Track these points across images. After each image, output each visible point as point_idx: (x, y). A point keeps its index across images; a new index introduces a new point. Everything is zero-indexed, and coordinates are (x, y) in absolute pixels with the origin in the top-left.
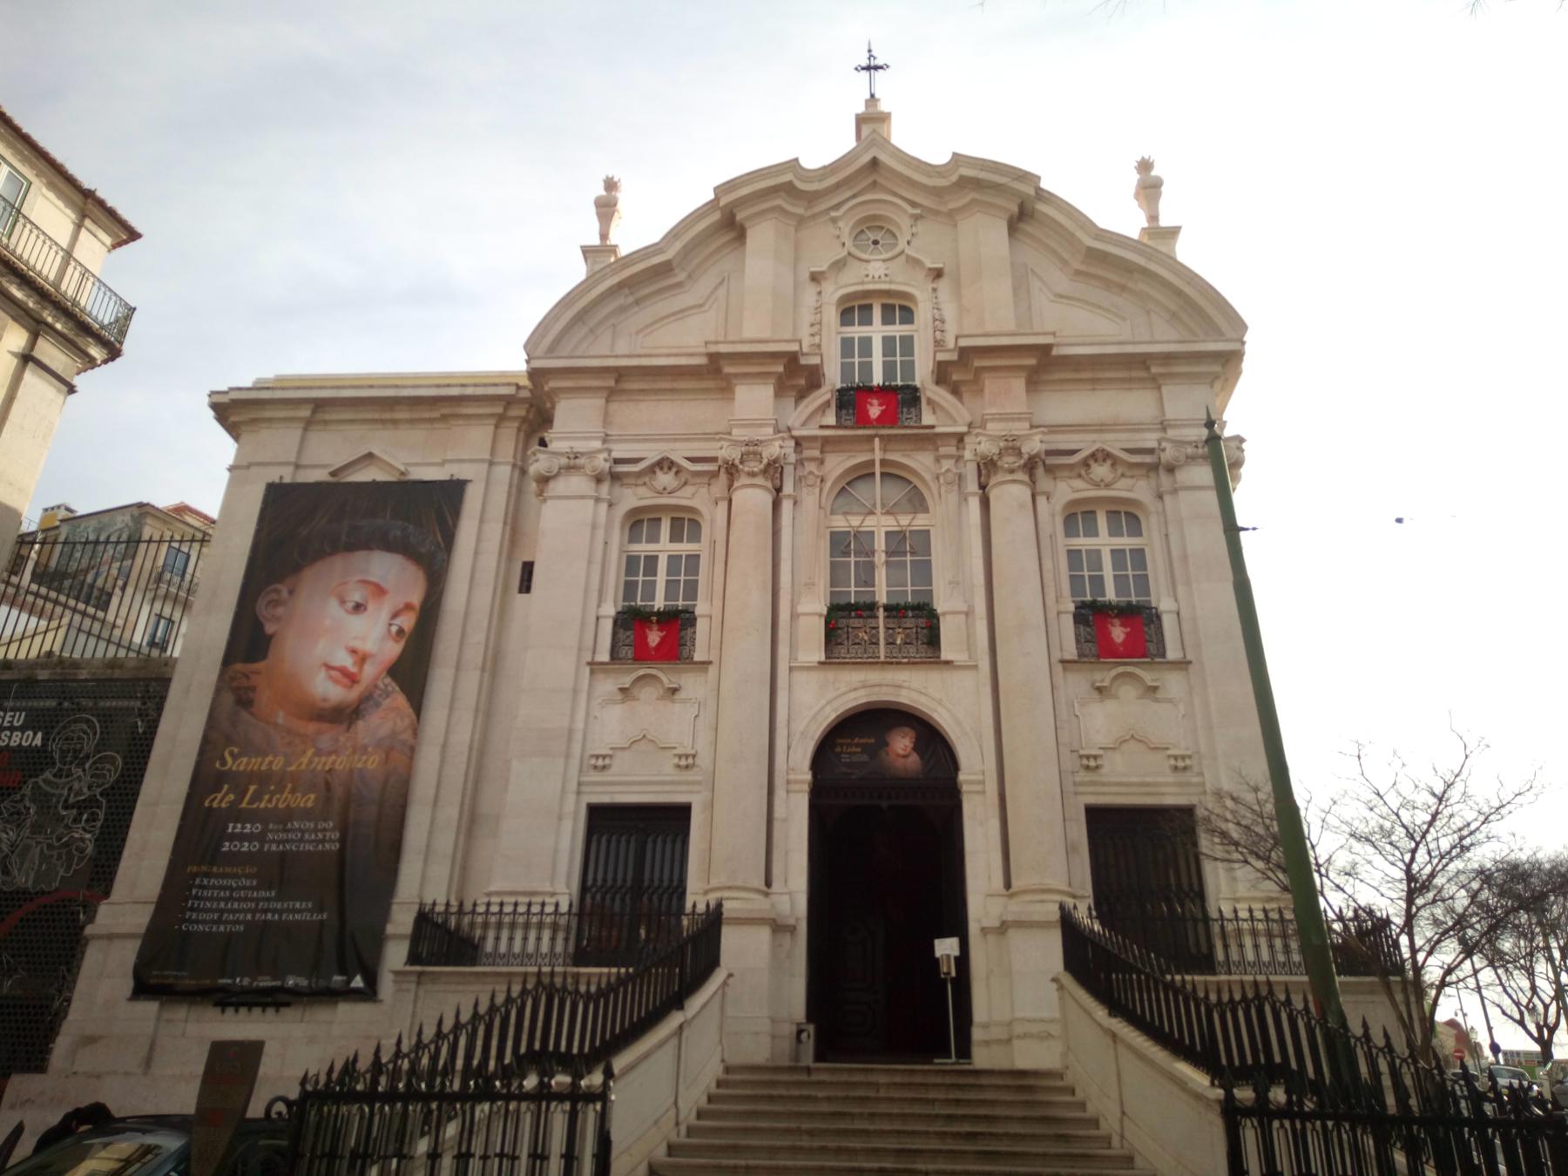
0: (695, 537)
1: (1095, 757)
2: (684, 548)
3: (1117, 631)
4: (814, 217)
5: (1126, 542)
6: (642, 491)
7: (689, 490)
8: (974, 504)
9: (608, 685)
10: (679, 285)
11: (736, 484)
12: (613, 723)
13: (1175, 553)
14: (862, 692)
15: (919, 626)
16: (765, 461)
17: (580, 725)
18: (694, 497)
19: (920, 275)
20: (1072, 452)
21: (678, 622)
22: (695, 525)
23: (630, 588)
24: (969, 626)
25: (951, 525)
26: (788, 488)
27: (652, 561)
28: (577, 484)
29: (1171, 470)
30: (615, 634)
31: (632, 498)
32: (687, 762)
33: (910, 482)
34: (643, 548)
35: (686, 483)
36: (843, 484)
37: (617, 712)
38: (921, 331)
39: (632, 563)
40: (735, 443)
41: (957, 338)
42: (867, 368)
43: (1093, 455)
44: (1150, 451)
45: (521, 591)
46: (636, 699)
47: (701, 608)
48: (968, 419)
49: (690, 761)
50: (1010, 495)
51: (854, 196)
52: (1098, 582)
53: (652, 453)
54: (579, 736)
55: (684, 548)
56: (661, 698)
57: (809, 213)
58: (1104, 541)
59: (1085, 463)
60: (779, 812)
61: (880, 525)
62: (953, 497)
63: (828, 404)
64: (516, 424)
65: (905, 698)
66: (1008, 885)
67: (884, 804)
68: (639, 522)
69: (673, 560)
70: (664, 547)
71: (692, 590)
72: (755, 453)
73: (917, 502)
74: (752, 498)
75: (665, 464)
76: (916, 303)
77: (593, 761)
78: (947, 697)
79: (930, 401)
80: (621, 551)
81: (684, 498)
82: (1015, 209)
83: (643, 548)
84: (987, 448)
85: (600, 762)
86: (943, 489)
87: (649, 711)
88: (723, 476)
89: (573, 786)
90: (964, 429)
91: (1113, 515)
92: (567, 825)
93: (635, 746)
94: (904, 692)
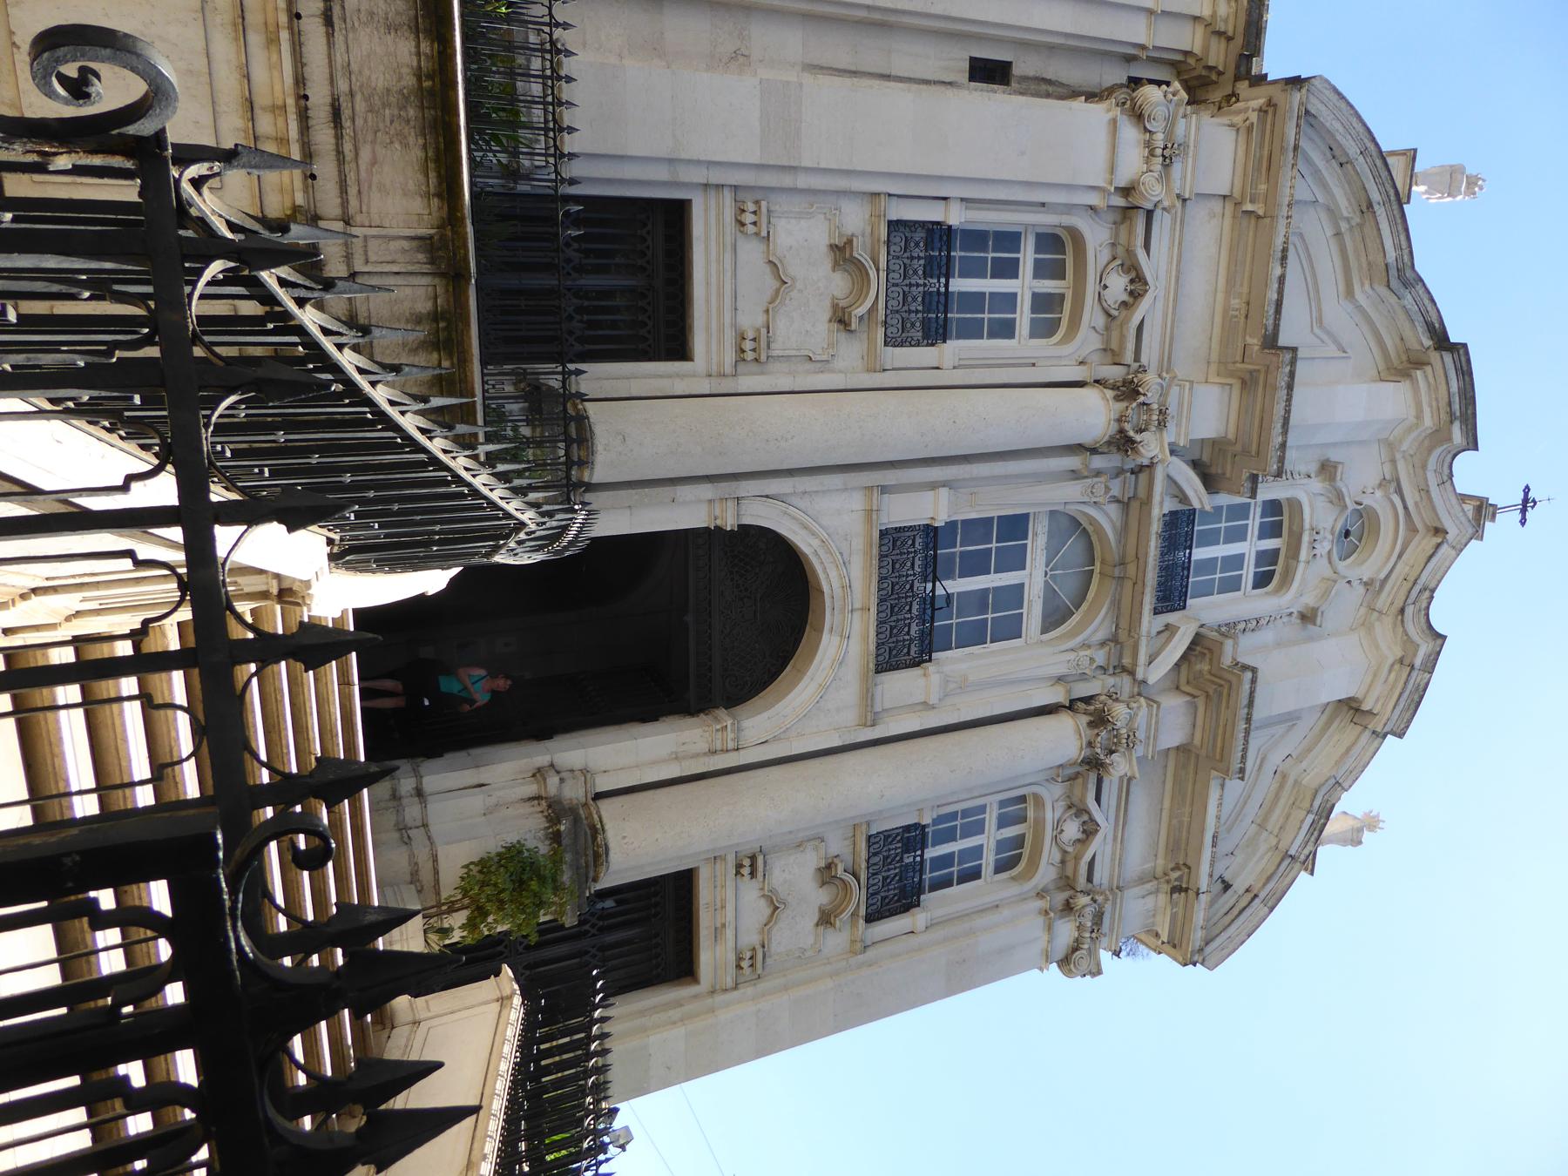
1: (753, 874)
2: (1023, 316)
3: (897, 873)
4: (1393, 461)
5: (988, 861)
6: (1105, 256)
7: (1100, 321)
8: (1056, 695)
9: (855, 219)
10: (1350, 293)
11: (1110, 394)
13: (979, 922)
14: (836, 584)
15: (909, 636)
16: (1138, 438)
17: (802, 181)
19: (1309, 600)
20: (1098, 799)
21: (930, 319)
23: (976, 238)
24: (912, 708)
25: (1030, 664)
29: (1068, 908)
30: (923, 224)
31: (1097, 237)
32: (752, 350)
33: (1078, 607)
34: (1028, 256)
35: (1109, 315)
36: (1085, 524)
38: (1246, 603)
39: (1010, 240)
40: (1164, 394)
41: (1254, 670)
42: (1211, 539)
43: (1092, 820)
44: (1090, 879)
45: (973, 60)
46: (836, 266)
47: (953, 349)
48: (1152, 680)
49: (750, 356)
50: (1062, 739)
51: (1406, 508)
52: (949, 836)
53: (1155, 266)
54: (787, 180)
55: (1023, 316)
56: (835, 307)
57: (1398, 456)
58: (989, 839)
59: (1080, 810)
60: (685, 492)
61: (1033, 578)
62: (1062, 670)
63: (1183, 498)
64: (1197, 50)
66: (599, 796)
67: (689, 618)
69: (1009, 300)
72: (1148, 423)
73: (1055, 617)
75: (1138, 285)
76: (1277, 591)
77: (751, 207)
79: (1169, 629)
80: (1027, 226)
81: (1092, 316)
82: (1365, 707)
83: (1028, 256)
84: (1120, 712)
85: (748, 218)
86: (1072, 656)
87: (822, 283)
88: (1114, 373)
89: (716, 177)
90: (1140, 676)
91: (1019, 841)
92: (662, 173)
93: (768, 269)
94: (836, 640)
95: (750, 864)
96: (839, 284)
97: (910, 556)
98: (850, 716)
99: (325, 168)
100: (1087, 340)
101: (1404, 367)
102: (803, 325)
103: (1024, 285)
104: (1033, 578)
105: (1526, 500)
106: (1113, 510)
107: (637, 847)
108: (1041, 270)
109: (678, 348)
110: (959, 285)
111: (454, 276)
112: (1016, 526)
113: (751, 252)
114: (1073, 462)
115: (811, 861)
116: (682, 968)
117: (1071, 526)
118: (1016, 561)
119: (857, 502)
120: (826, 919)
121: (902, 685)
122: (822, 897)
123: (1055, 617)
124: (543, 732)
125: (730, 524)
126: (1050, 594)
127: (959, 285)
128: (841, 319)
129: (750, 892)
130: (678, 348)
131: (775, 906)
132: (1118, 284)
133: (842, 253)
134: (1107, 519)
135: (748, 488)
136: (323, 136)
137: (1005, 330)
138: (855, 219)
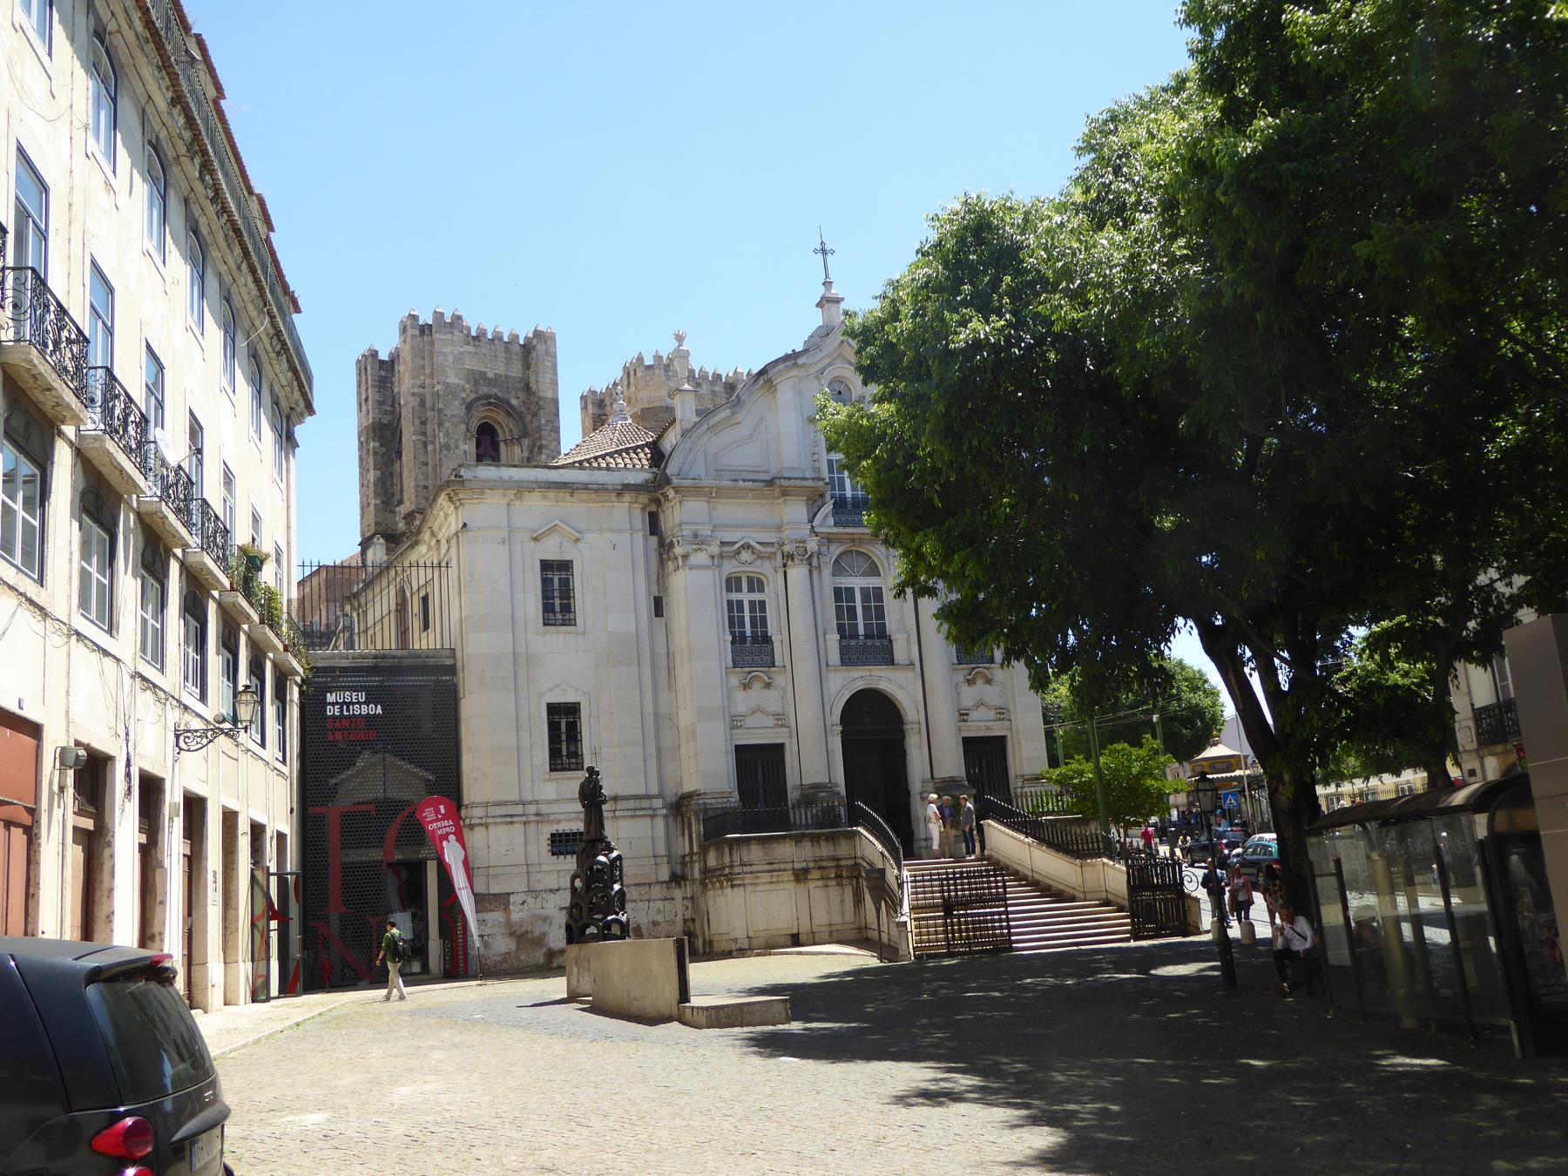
0: (761, 590)
2: (757, 596)
6: (734, 561)
12: (743, 702)
18: (765, 569)
22: (761, 583)
26: (815, 562)
27: (740, 603)
28: (701, 558)
31: (730, 567)
32: (781, 720)
37: (740, 695)
39: (730, 603)
55: (757, 596)
61: (857, 583)
65: (883, 686)
68: (732, 584)
69: (752, 603)
70: (746, 597)
71: (764, 619)
73: (874, 570)
74: (798, 573)
78: (896, 683)
83: (735, 596)
95: (963, 715)
96: (756, 686)
97: (852, 655)
98: (910, 674)
99: (782, 866)
100: (765, 569)
101: (770, 386)
102: (771, 700)
103: (746, 597)
104: (857, 583)
105: (824, 252)
106: (832, 548)
107: (952, 764)
108: (739, 590)
109: (781, 747)
110: (748, 633)
111: (803, 836)
112: (838, 592)
113: (749, 722)
114: (815, 574)
115: (965, 689)
116: (1000, 742)
117: (838, 569)
118: (850, 591)
119: (831, 676)
120: (989, 681)
121: (900, 653)
122: (980, 682)
123: (874, 570)
124: (908, 793)
125: (840, 728)
126: (865, 574)
127: (748, 633)
128: (768, 686)
129: (974, 715)
130: (781, 747)
131: (980, 704)
132: (746, 556)
133: (746, 686)
134: (836, 550)
135: (829, 724)
136: (775, 867)
137: (762, 604)
138: (734, 680)
